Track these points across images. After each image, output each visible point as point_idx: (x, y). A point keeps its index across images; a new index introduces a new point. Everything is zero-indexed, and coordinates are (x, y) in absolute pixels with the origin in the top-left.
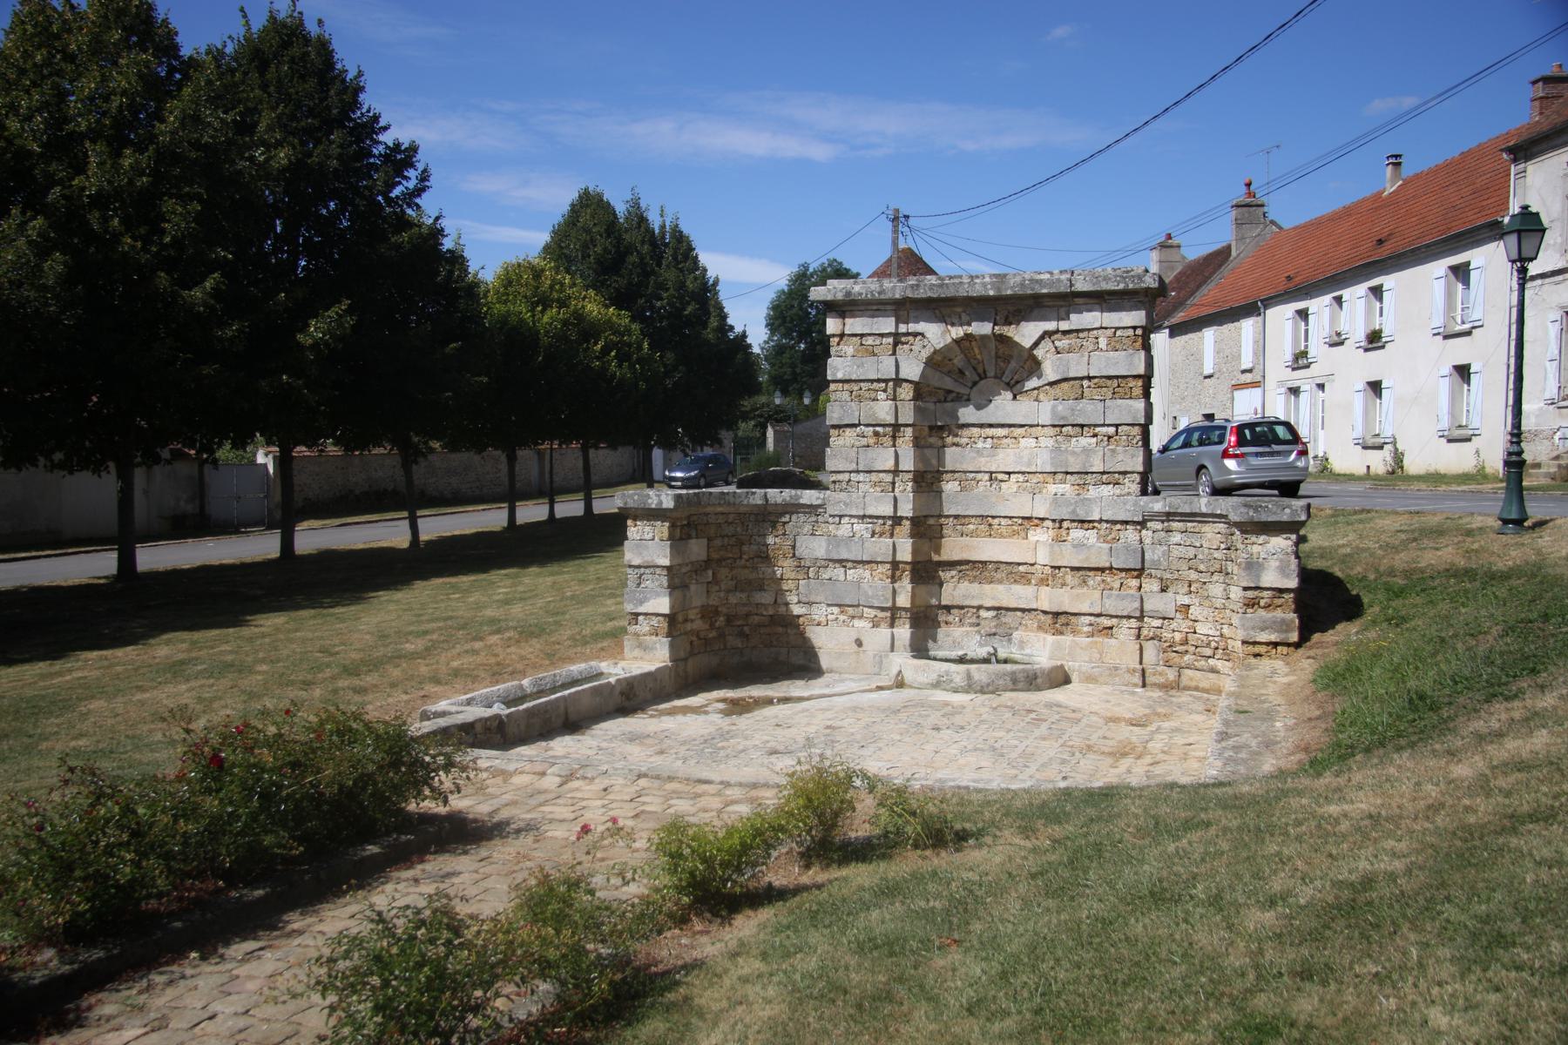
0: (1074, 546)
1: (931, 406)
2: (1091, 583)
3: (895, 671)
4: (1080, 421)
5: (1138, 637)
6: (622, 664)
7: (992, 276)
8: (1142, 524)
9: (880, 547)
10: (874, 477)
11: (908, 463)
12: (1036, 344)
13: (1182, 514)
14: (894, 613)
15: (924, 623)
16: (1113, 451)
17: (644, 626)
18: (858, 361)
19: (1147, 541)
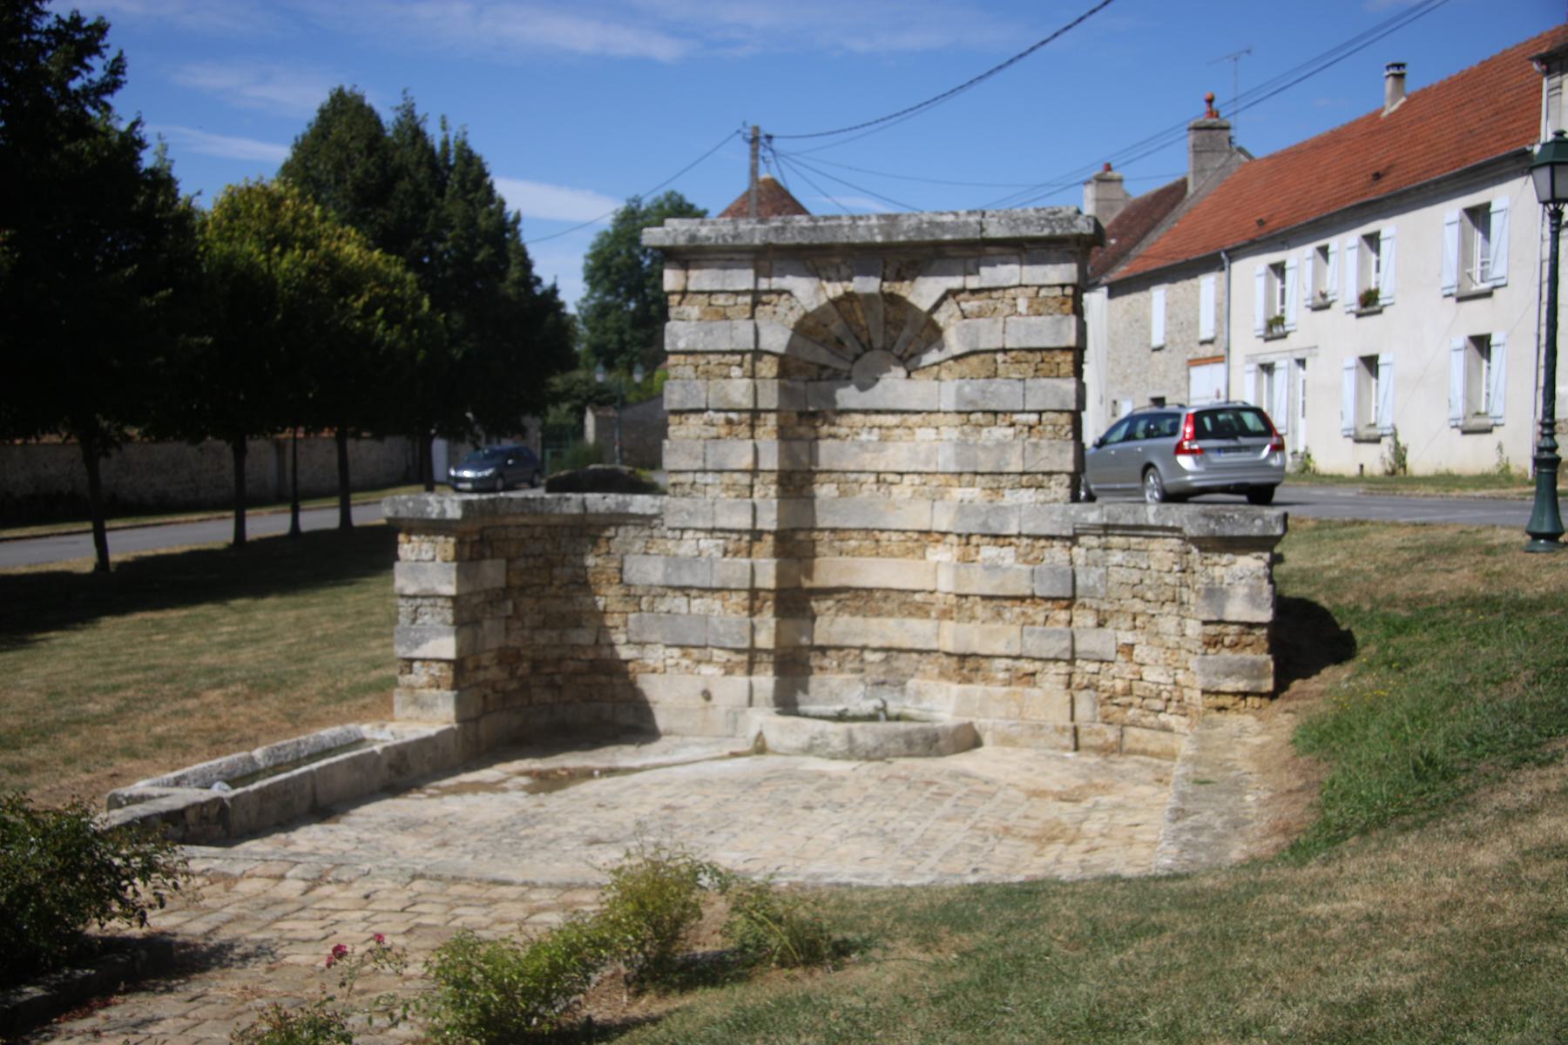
0: (986, 568)
1: (800, 386)
2: (1007, 615)
3: (753, 733)
4: (993, 406)
5: (1069, 685)
6: (391, 726)
7: (880, 216)
8: (1073, 539)
9: (735, 570)
10: (726, 478)
11: (770, 461)
12: (937, 306)
14: (752, 658)
15: (793, 669)
16: (1036, 445)
17: (420, 675)
19: (1080, 561)
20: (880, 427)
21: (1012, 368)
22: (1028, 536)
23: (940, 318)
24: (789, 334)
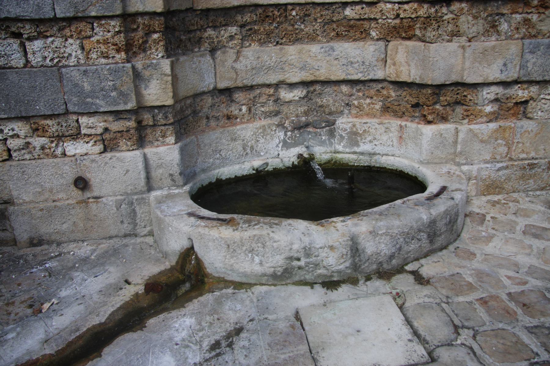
2: (504, 27)
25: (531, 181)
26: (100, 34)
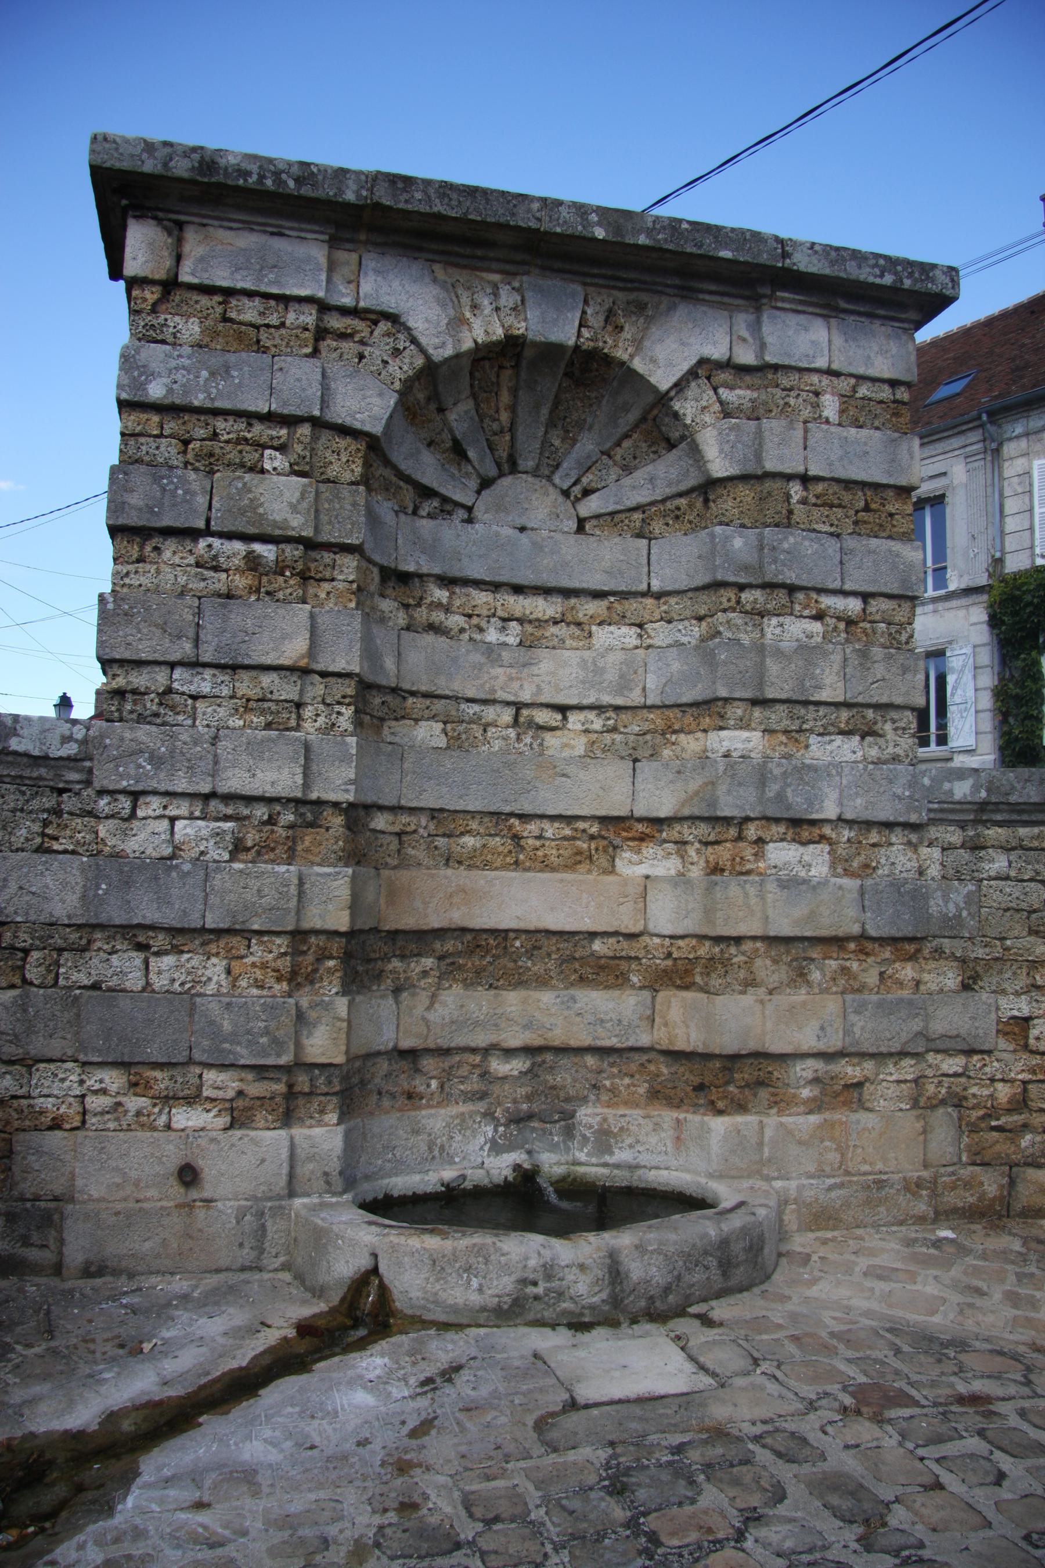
2: (816, 976)
4: (790, 576)
9: (262, 887)
10: (245, 685)
12: (680, 386)
13: (1016, 808)
18: (216, 360)
20: (520, 621)
21: (816, 513)
22: (850, 823)
23: (687, 408)
24: (392, 400)
25: (882, 1209)
26: (258, 953)
